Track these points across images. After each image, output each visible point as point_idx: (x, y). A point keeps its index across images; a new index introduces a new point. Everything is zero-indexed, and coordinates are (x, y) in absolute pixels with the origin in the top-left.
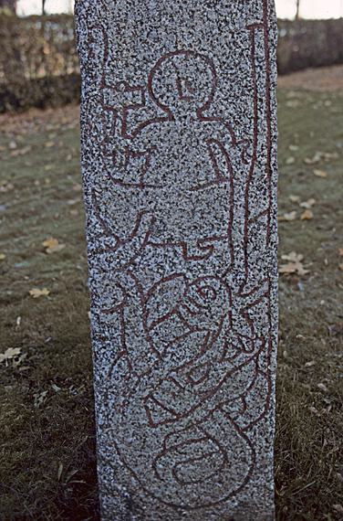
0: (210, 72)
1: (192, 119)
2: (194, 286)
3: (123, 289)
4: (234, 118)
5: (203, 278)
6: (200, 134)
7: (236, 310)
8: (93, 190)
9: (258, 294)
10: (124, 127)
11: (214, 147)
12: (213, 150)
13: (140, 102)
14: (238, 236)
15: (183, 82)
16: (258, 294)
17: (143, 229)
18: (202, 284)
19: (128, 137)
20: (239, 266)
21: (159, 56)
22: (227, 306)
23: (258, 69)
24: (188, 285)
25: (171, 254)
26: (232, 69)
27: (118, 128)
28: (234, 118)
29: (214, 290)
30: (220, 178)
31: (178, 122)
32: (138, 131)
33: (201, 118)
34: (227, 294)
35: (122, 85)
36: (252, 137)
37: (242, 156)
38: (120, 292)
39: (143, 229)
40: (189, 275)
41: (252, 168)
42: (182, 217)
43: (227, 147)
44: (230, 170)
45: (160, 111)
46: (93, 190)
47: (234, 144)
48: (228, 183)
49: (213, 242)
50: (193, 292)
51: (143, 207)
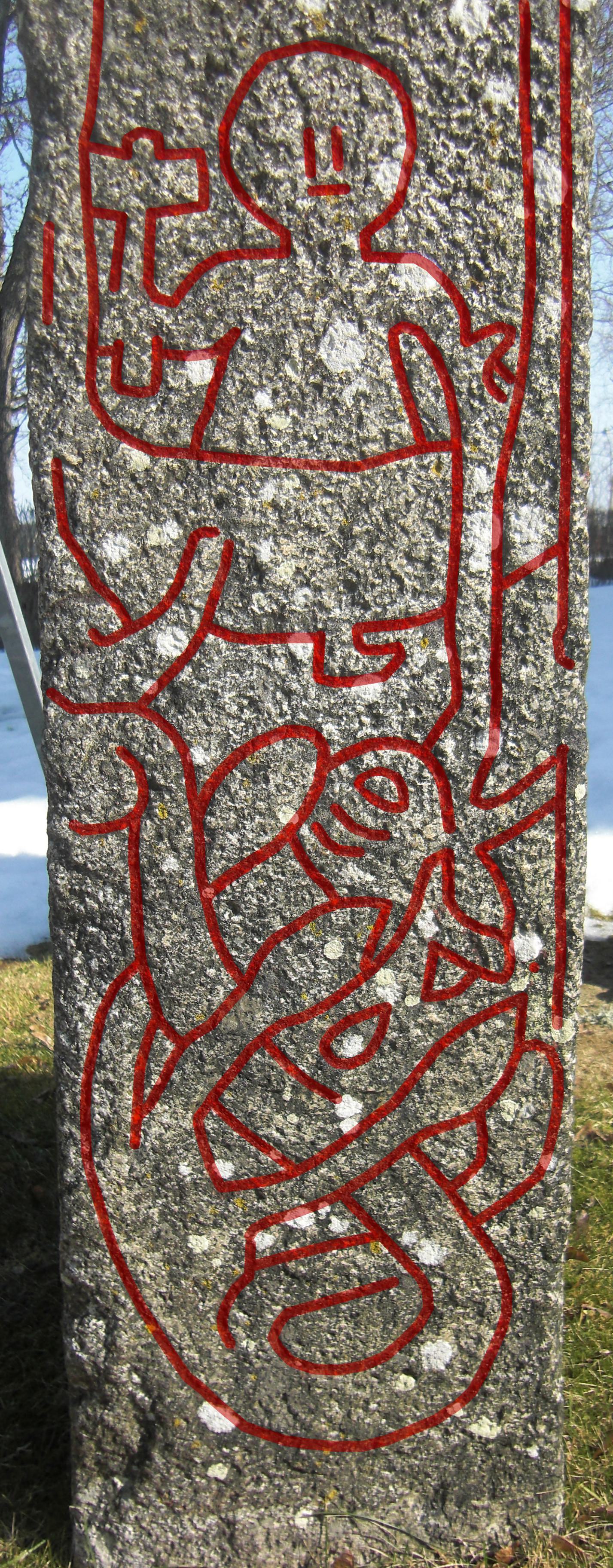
0: (398, 112)
1: (346, 254)
2: (343, 768)
3: (138, 765)
4: (467, 258)
5: (371, 744)
6: (369, 302)
7: (465, 846)
8: (59, 461)
9: (528, 802)
10: (150, 270)
11: (407, 343)
12: (404, 349)
13: (194, 195)
14: (474, 619)
15: (321, 140)
16: (528, 802)
17: (202, 581)
18: (369, 760)
19: (160, 300)
20: (476, 712)
21: (249, 50)
22: (437, 830)
23: (540, 111)
24: (326, 762)
25: (280, 665)
26: (461, 104)
27: (134, 268)
28: (467, 258)
29: (400, 781)
30: (423, 444)
31: (303, 261)
32: (192, 281)
33: (370, 253)
34: (436, 795)
35: (146, 141)
36: (517, 319)
37: (488, 373)
38: (128, 776)
39: (202, 581)
40: (330, 729)
41: (516, 413)
42: (311, 552)
43: (445, 343)
44: (455, 414)
45: (254, 224)
46: (59, 461)
47: (469, 337)
48: (447, 457)
49: (400, 634)
50: (341, 787)
51: (202, 515)
